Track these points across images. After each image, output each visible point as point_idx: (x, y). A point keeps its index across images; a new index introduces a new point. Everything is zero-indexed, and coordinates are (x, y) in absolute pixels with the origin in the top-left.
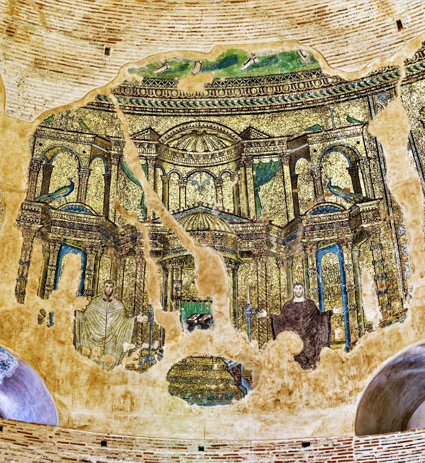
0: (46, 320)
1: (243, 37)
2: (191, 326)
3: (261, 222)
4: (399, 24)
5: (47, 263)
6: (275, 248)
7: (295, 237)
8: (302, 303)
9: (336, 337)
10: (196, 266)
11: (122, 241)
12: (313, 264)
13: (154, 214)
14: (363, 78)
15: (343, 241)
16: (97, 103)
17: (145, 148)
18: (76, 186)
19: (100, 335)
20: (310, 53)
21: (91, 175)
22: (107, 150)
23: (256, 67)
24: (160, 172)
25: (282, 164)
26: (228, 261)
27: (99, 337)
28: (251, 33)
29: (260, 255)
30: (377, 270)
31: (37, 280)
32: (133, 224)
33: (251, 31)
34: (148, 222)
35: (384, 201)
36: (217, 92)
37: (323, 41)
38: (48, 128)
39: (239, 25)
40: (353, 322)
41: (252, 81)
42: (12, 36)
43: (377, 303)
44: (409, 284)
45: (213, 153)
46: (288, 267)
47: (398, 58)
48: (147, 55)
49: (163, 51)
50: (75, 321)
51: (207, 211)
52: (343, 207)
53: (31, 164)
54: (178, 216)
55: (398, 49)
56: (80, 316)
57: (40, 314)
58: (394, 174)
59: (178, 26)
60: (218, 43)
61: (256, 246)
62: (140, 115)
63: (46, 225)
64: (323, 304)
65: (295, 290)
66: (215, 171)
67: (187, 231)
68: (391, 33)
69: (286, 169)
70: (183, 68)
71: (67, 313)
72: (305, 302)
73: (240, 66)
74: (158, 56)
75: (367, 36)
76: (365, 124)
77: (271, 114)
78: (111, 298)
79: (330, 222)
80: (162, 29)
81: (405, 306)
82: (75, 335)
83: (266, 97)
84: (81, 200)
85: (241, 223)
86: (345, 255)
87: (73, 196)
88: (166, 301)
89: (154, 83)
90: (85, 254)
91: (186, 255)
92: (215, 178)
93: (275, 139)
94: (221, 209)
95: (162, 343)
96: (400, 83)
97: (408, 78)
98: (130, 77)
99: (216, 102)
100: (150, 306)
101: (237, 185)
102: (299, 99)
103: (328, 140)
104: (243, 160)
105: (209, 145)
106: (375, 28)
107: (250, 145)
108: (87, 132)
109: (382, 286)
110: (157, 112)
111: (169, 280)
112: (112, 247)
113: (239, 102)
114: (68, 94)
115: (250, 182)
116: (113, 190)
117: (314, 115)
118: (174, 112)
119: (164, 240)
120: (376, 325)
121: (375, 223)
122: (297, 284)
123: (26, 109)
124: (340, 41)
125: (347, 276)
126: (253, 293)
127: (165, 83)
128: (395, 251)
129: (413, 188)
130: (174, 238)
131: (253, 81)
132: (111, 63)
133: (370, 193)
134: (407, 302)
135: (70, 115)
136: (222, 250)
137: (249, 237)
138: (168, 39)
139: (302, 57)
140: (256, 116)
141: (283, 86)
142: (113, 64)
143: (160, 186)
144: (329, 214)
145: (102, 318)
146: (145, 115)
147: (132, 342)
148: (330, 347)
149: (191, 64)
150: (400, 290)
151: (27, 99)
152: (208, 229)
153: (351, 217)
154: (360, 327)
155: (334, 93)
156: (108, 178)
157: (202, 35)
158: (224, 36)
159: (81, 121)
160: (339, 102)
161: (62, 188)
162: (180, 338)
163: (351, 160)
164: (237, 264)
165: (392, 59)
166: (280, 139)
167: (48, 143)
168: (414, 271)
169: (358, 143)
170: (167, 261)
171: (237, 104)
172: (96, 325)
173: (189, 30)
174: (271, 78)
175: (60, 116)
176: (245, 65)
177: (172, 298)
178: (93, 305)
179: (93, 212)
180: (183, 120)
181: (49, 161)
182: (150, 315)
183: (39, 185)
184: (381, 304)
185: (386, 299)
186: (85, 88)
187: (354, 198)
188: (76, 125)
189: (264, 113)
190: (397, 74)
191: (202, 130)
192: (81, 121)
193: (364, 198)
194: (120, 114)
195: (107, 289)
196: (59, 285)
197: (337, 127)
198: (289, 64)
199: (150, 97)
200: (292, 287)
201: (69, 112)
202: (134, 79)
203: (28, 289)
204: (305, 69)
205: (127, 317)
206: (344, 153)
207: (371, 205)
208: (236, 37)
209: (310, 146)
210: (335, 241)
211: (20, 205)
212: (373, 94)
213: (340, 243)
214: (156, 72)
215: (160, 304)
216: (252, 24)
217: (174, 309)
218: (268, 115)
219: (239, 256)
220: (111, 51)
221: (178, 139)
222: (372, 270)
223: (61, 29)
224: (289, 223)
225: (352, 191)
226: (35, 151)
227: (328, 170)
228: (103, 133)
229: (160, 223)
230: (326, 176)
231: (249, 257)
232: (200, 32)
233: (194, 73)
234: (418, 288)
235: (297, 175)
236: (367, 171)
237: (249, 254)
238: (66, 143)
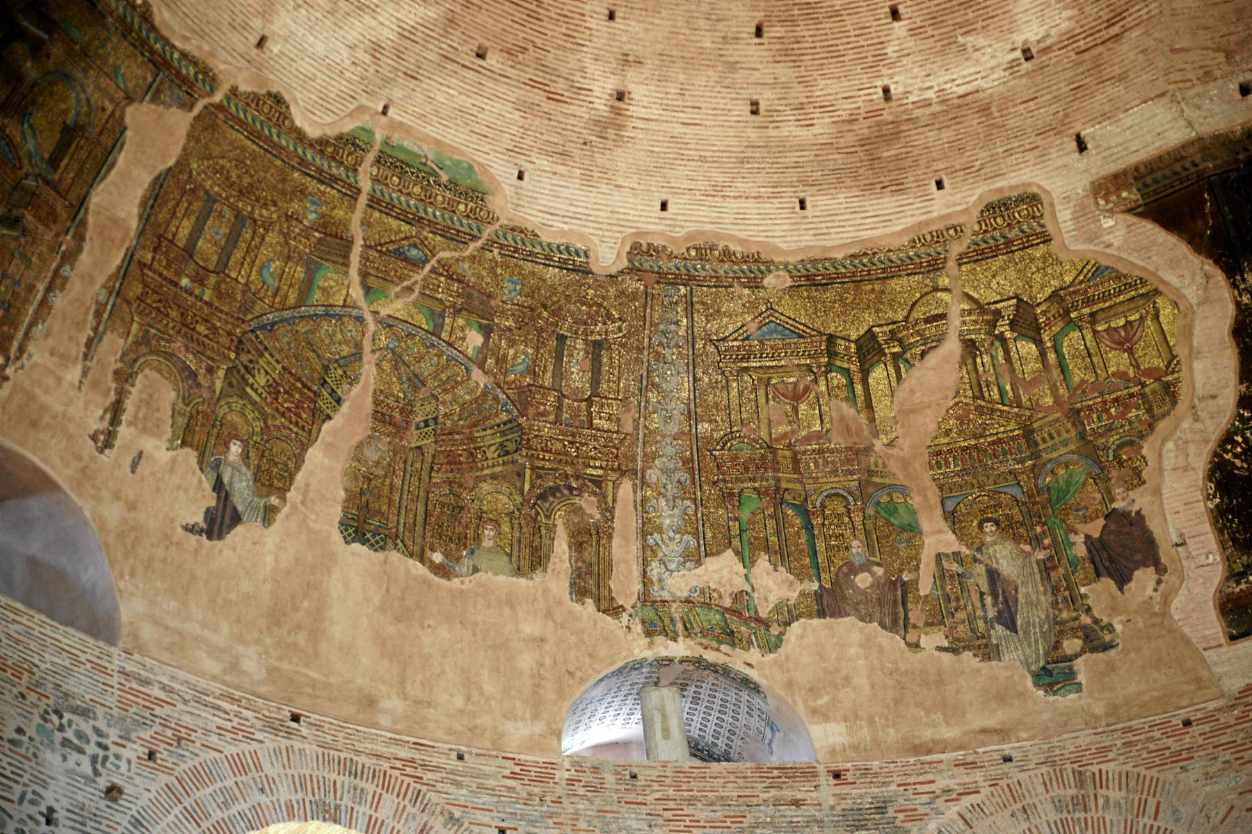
4: (261, 42)
14: (173, 46)
44: (31, 348)
47: (230, 73)
52: (20, 161)
58: (110, 194)
76: (130, 99)
81: (9, 371)
97: (219, 107)
106: (237, 12)
121: (41, 227)
128: (41, 287)
129: (118, 235)
134: (13, 368)
150: (15, 344)
160: (125, 37)
165: (222, 67)
168: (47, 336)
190: (212, 90)
225: (46, 155)
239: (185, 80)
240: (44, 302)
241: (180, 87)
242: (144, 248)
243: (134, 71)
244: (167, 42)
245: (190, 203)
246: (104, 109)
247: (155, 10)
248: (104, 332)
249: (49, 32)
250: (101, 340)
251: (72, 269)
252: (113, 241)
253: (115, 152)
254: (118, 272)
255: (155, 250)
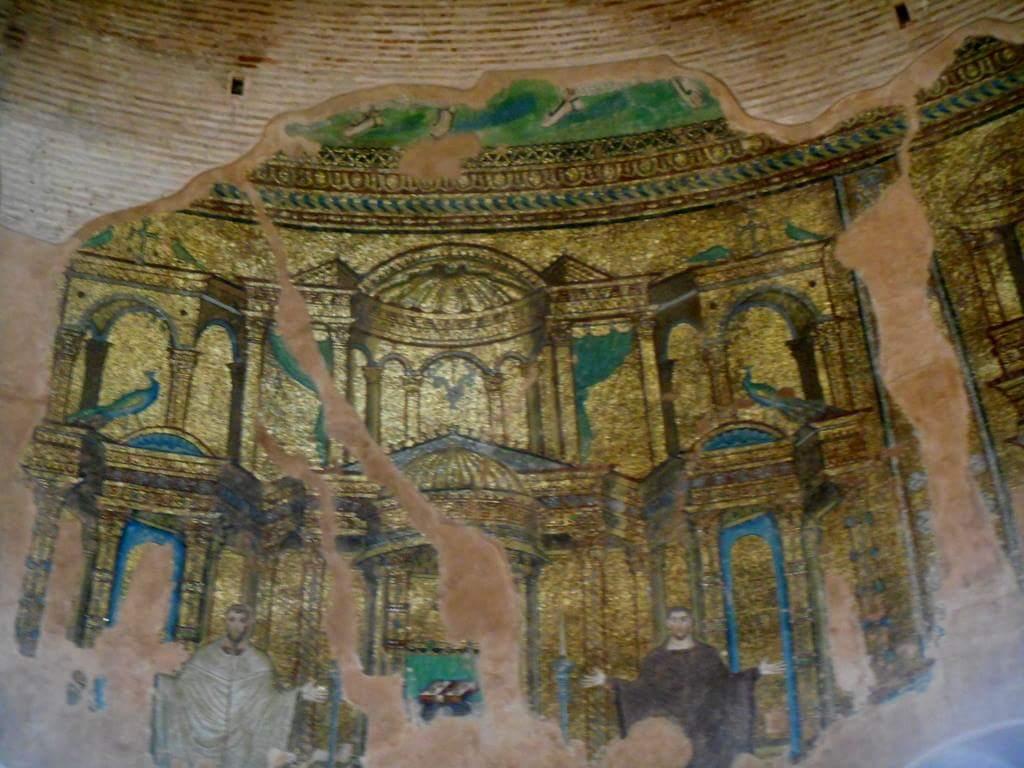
0: (87, 696)
1: (548, 51)
2: (428, 706)
3: (589, 468)
5: (92, 565)
6: (623, 526)
7: (665, 502)
8: (685, 653)
9: (770, 731)
10: (443, 570)
11: (270, 517)
12: (711, 564)
13: (346, 454)
14: (822, 138)
15: (779, 509)
16: (213, 202)
17: (324, 305)
18: (164, 388)
19: (216, 731)
20: (700, 84)
21: (200, 364)
22: (236, 307)
23: (575, 121)
24: (360, 359)
25: (635, 337)
26: (520, 557)
27: (212, 736)
28: (566, 43)
29: (589, 542)
30: (863, 573)
31: (68, 604)
32: (296, 476)
33: (566, 38)
34: (332, 471)
35: (872, 415)
36: (489, 178)
37: (731, 57)
38: (99, 256)
39: (539, 24)
40: (809, 695)
41: (569, 151)
42: (16, 47)
43: (863, 650)
44: (938, 602)
45: (480, 315)
46: (654, 571)
48: (329, 95)
49: (364, 86)
50: (154, 699)
51: (466, 445)
53: (59, 340)
54: (401, 456)
55: (902, 68)
56: (166, 688)
57: (74, 683)
59: (400, 28)
60: (492, 67)
61: (580, 523)
62: (314, 229)
63: (90, 478)
64: (738, 653)
65: (670, 623)
66: (486, 355)
67: (424, 491)
68: (883, 33)
69: (648, 350)
70: (413, 122)
71: (139, 681)
72: (694, 649)
73: (539, 118)
74: (353, 96)
75: (829, 43)
76: (826, 241)
77: (611, 227)
78: (241, 646)
79: (749, 466)
80: (361, 36)
81: (929, 653)
82: (154, 731)
83: (600, 188)
84: (174, 421)
85: (544, 472)
86: (786, 541)
87: (155, 411)
88: (370, 652)
89: (346, 159)
90: (183, 546)
91: (420, 547)
92: (485, 373)
93: (621, 282)
94: (499, 440)
95: (360, 749)
96: (906, 144)
97: (926, 131)
98: (287, 141)
99: (488, 201)
100: (333, 663)
101: (536, 387)
102: (675, 190)
103: (743, 280)
104: (549, 330)
105: (472, 298)
107: (565, 296)
108: (191, 267)
109: (874, 610)
110: (352, 223)
111: (379, 603)
112: (245, 527)
113: (539, 201)
114: (147, 182)
115: (565, 379)
116: (249, 400)
117: (710, 225)
118: (391, 224)
119: (368, 512)
120: (861, 699)
121: (855, 467)
122: (676, 609)
123: (49, 213)
124: (770, 55)
125: (792, 588)
126: (575, 628)
127: (370, 157)
128: (903, 529)
130: (393, 508)
131: (570, 151)
132: (245, 112)
133: (842, 398)
135: (150, 229)
136: (502, 532)
137: (564, 502)
138: (376, 58)
139: (682, 93)
140: (576, 231)
141: (639, 162)
142: (251, 113)
143: (360, 394)
144: (748, 448)
145: (220, 692)
146: (326, 230)
147: (290, 748)
148: (751, 752)
149: (430, 116)
150: (917, 616)
151: (52, 191)
152: (470, 487)
153: (796, 453)
154: (823, 705)
155: (755, 173)
156: (238, 372)
157: (454, 50)
158: (504, 51)
159: (176, 242)
160: (768, 194)
161: (131, 395)
162: (402, 737)
163: (797, 324)
164: (536, 563)
165: (887, 92)
166: (632, 281)
167: (98, 291)
169: (812, 284)
170: (377, 559)
171: (536, 205)
172: (204, 708)
173: (424, 38)
174: (615, 145)
175: (127, 230)
176: (552, 114)
177: (386, 644)
178: (198, 663)
179: (204, 450)
180: (412, 240)
181: (101, 332)
182: (332, 684)
183: (77, 385)
184: (873, 651)
185: (884, 639)
186: (183, 167)
187: (806, 410)
188: (164, 250)
189: (594, 224)
190: (901, 127)
191: (455, 265)
192: (176, 242)
193: (828, 409)
194: (266, 229)
195: (233, 625)
196: (119, 615)
197: (765, 250)
198: (652, 110)
199: (336, 190)
200: (663, 614)
201: (147, 222)
202: (299, 147)
203: (45, 623)
204: (689, 120)
205: (279, 688)
206: (780, 308)
207: (844, 425)
208: (532, 53)
209: (702, 294)
210: (762, 509)
211: (30, 432)
212: (845, 173)
213: (774, 512)
214: (350, 132)
215: (356, 658)
216: (568, 21)
217: (389, 667)
218: (606, 229)
219: (540, 546)
220: (247, 85)
221: (402, 284)
222: (849, 573)
223: (132, 34)
224: (655, 469)
225: (800, 394)
226: (68, 309)
227: (745, 345)
228: (228, 269)
229: (358, 473)
230: (740, 363)
231: (564, 548)
232: (449, 41)
233: (437, 134)
234: (958, 611)
235: (671, 363)
236: (834, 348)
237: (563, 540)
238: (140, 292)
239: (863, 154)
240: (917, 539)
241: (868, 165)
242: (980, 364)
243: (809, 212)
244: (811, 142)
245: (987, 262)
246: (812, 284)
247: (771, 132)
248: (1009, 500)
249: (692, 285)
250: (1010, 512)
251: (922, 473)
252: (942, 395)
253: (866, 309)
254: (975, 420)
255: (995, 353)
